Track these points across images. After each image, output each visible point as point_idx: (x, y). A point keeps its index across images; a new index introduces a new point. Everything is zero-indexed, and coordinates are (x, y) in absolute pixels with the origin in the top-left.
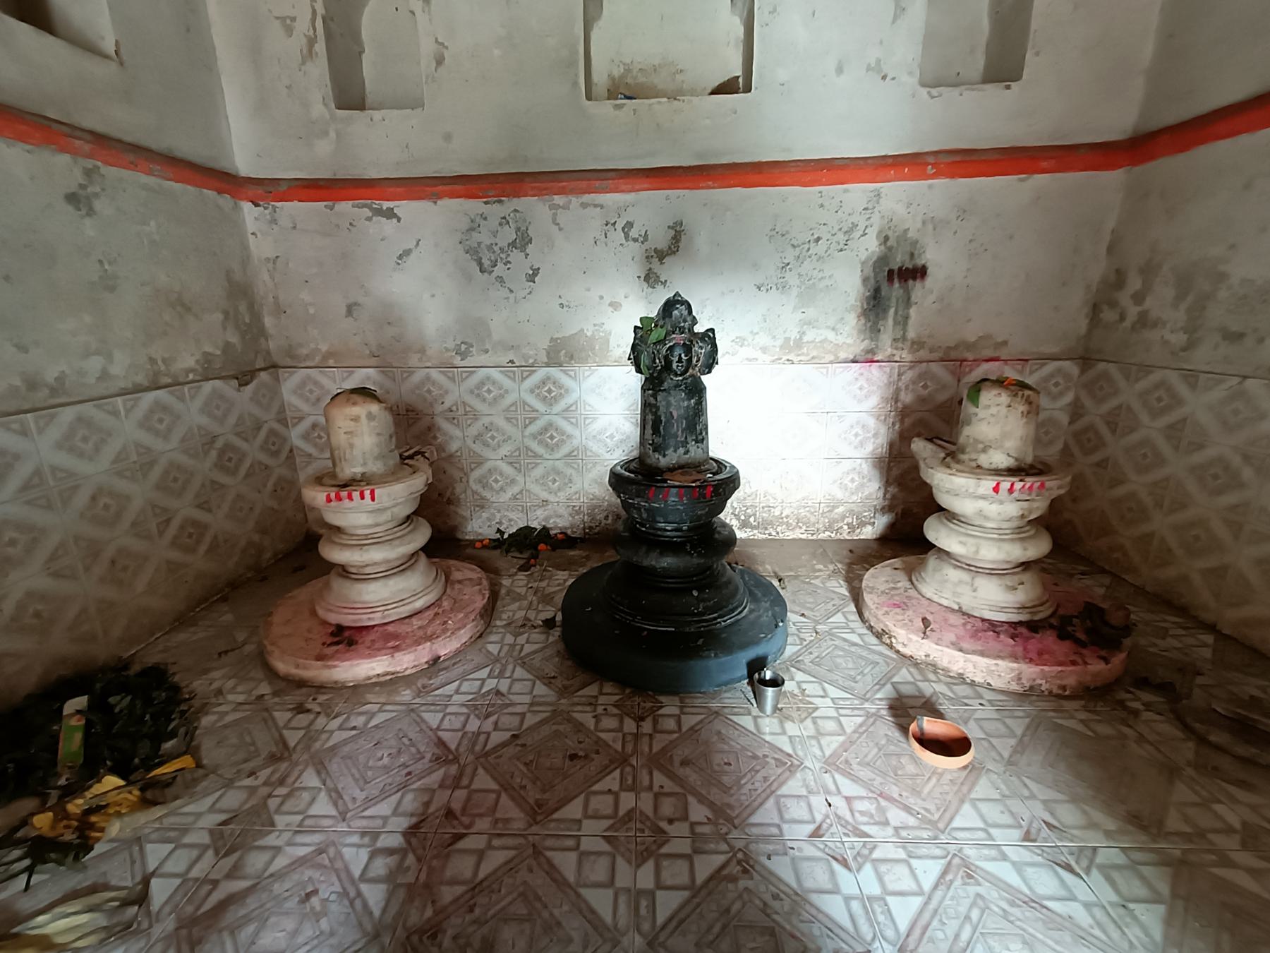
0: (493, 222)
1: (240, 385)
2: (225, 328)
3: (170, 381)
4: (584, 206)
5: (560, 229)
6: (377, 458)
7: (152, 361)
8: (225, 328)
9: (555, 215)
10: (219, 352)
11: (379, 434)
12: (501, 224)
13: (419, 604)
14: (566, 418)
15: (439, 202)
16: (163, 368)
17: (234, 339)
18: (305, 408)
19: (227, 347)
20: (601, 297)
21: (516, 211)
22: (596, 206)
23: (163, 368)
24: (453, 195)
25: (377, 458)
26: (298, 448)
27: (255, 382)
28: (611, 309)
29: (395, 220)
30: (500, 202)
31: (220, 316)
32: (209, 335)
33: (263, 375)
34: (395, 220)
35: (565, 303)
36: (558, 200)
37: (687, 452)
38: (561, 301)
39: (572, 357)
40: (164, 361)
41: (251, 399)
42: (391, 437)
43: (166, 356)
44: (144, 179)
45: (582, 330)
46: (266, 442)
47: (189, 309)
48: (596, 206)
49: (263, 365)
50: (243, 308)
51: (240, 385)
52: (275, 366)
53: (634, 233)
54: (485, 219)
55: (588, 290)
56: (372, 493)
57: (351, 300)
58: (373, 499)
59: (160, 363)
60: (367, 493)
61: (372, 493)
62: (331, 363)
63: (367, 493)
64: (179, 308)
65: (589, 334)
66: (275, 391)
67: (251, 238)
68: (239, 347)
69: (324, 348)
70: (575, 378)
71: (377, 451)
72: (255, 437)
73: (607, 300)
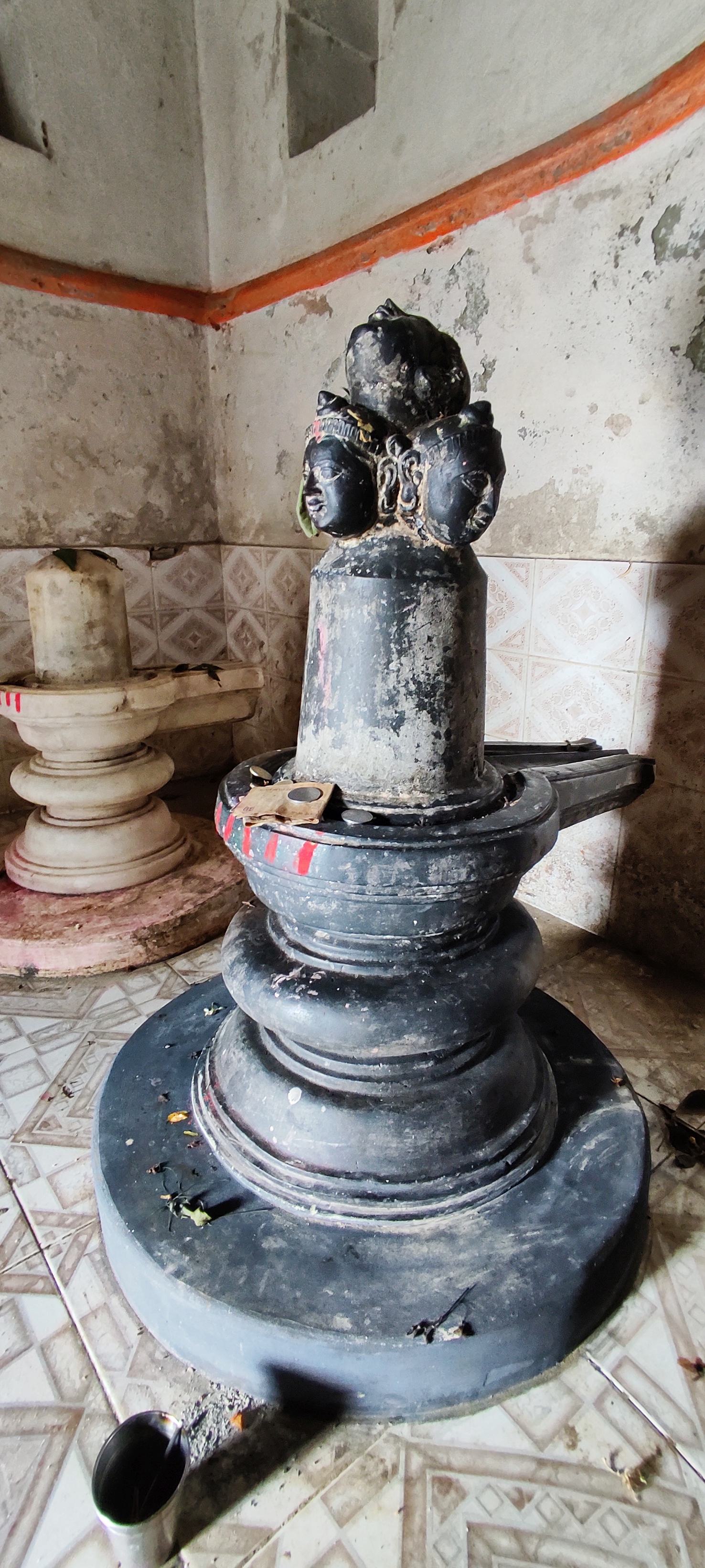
0: (439, 280)
1: (153, 558)
2: (148, 488)
3: (51, 541)
4: (582, 202)
5: (535, 271)
6: (61, 653)
7: (30, 516)
8: (148, 488)
9: (529, 240)
10: (130, 515)
11: (67, 619)
12: (448, 285)
13: (81, 884)
14: (505, 659)
15: (374, 269)
16: (44, 525)
17: (160, 500)
18: (238, 597)
19: (146, 511)
20: (593, 408)
21: (470, 252)
22: (603, 195)
23: (44, 525)
24: (390, 250)
25: (61, 653)
26: (231, 651)
27: (178, 557)
28: (609, 432)
29: (327, 314)
30: (447, 242)
31: (143, 472)
32: (132, 491)
33: (195, 551)
34: (327, 314)
35: (530, 427)
36: (537, 205)
37: (338, 743)
38: (522, 424)
39: (528, 539)
40: (46, 518)
41: (169, 578)
42: (91, 625)
43: (51, 512)
44: (54, 300)
45: (552, 482)
46: (182, 633)
47: (94, 460)
48: (603, 195)
49: (201, 538)
50: (182, 462)
51: (153, 558)
52: (219, 541)
53: (679, 236)
54: (427, 282)
55: (571, 394)
56: (18, 697)
57: (280, 450)
58: (18, 708)
59: (40, 518)
60: (13, 697)
61: (18, 697)
62: (262, 539)
63: (13, 697)
64: (79, 458)
65: (562, 490)
66: (210, 574)
67: (211, 372)
68: (166, 514)
69: (258, 519)
70: (525, 582)
71: (61, 642)
72: (163, 627)
73: (603, 415)
